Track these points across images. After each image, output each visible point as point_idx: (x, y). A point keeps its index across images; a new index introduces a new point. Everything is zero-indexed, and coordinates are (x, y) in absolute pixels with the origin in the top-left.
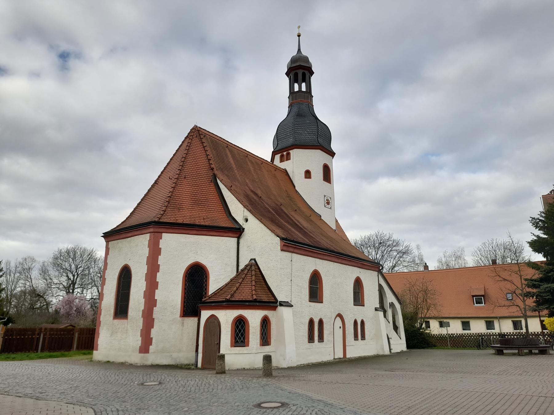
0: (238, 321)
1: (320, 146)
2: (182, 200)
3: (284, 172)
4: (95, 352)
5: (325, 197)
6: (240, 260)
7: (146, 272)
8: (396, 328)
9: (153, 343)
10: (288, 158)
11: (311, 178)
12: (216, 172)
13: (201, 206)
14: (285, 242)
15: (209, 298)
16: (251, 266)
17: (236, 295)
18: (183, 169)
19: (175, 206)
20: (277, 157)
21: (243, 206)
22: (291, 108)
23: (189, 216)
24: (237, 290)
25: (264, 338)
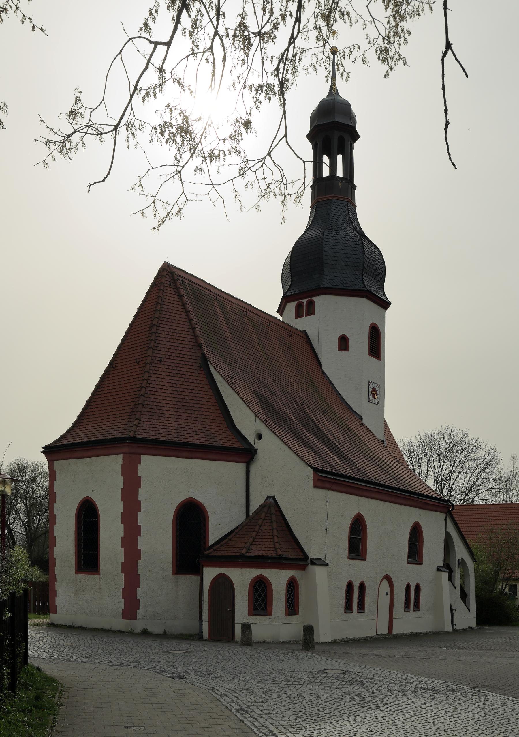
0: (257, 583)
5: (369, 384)
12: (207, 352)
13: (189, 411)
15: (214, 550)
16: (270, 507)
17: (253, 548)
18: (156, 347)
23: (175, 428)
24: (253, 541)
25: (290, 605)
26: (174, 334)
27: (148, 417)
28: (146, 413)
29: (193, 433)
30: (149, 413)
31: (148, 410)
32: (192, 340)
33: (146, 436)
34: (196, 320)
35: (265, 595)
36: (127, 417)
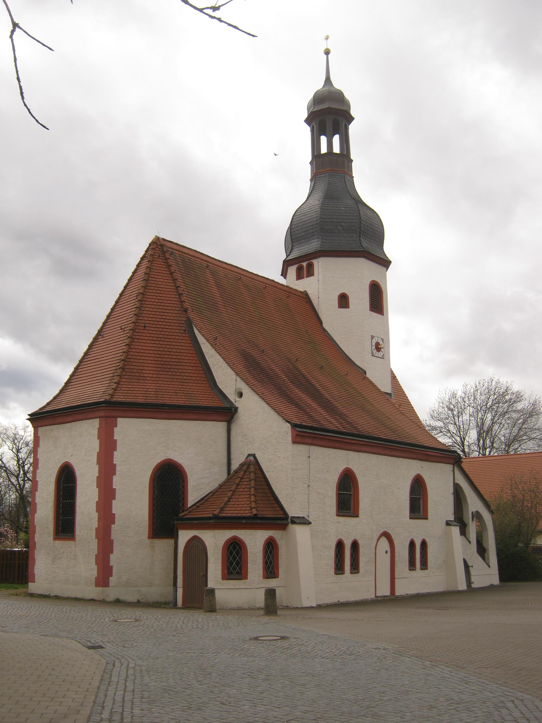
0: (231, 544)
1: (363, 251)
2: (142, 364)
3: (303, 298)
4: (30, 584)
6: (233, 456)
7: (97, 475)
8: (482, 551)
9: (114, 574)
10: (310, 272)
11: (349, 308)
12: (192, 315)
13: (170, 373)
14: (298, 431)
15: (190, 512)
16: (249, 465)
17: (228, 509)
18: (141, 314)
19: (132, 374)
20: (292, 271)
21: (234, 373)
22: (315, 183)
23: (154, 390)
24: (229, 501)
25: (269, 568)
26: (161, 301)
27: (128, 380)
28: (126, 377)
29: (172, 394)
30: (129, 377)
31: (129, 374)
32: (178, 306)
33: (123, 399)
34: (184, 287)
35: (240, 558)
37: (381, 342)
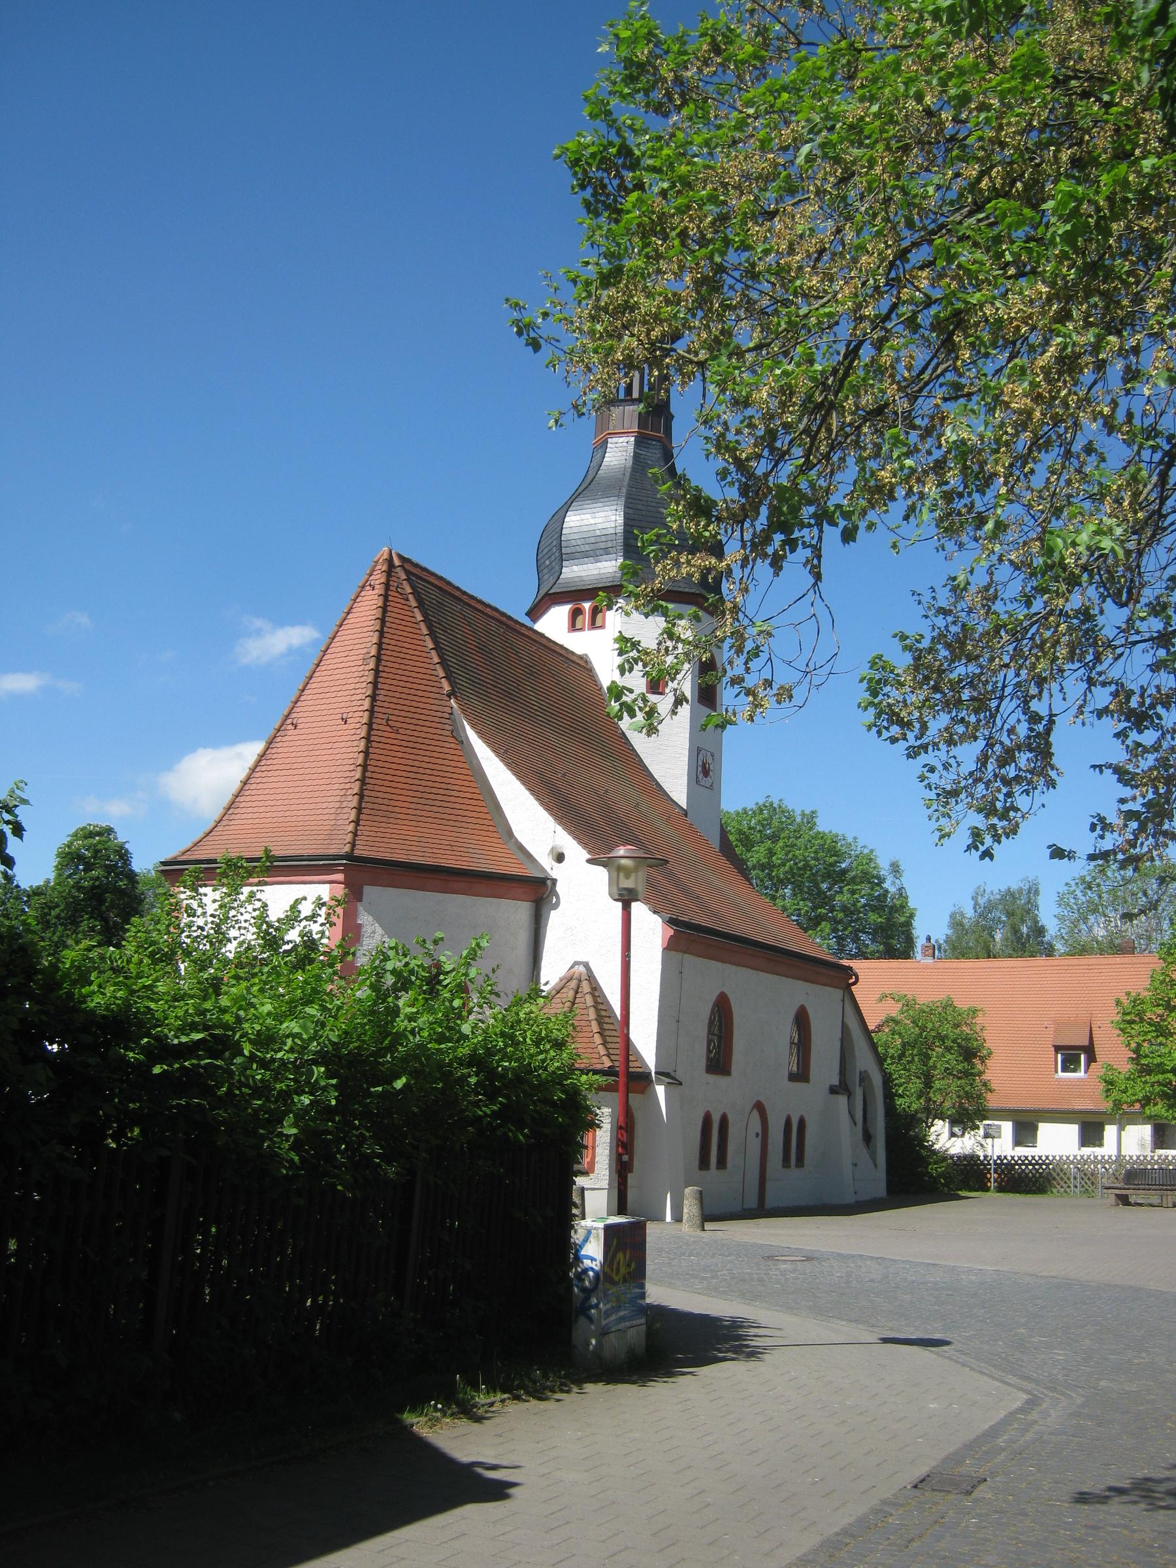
8: (868, 1137)
36: (332, 817)
37: (710, 761)
